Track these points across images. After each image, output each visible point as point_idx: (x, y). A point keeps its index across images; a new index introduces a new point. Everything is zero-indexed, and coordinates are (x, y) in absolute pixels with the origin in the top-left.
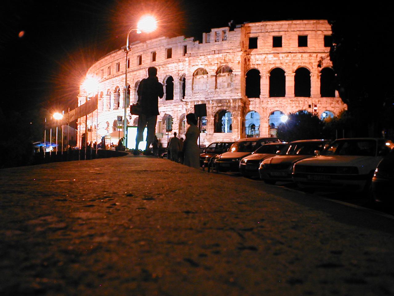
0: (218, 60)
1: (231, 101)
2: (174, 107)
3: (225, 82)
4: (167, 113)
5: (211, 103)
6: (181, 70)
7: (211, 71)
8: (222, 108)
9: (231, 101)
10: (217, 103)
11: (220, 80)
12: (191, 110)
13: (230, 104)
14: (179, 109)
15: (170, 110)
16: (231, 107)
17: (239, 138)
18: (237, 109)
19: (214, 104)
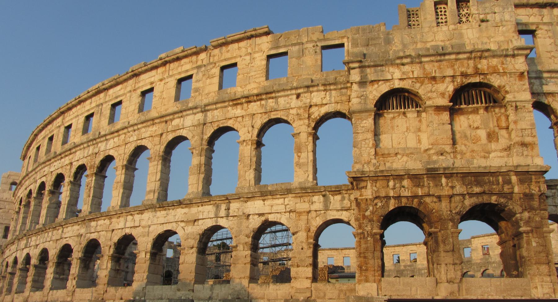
0: (454, 70)
1: (514, 179)
2: (298, 200)
3: (477, 128)
4: (271, 218)
5: (444, 184)
6: (316, 105)
7: (435, 95)
8: (485, 199)
9: (514, 179)
10: (467, 186)
11: (462, 122)
12: (376, 204)
13: (513, 188)
14: (314, 207)
15: (282, 208)
16: (516, 197)
18: (536, 204)
19: (458, 187)
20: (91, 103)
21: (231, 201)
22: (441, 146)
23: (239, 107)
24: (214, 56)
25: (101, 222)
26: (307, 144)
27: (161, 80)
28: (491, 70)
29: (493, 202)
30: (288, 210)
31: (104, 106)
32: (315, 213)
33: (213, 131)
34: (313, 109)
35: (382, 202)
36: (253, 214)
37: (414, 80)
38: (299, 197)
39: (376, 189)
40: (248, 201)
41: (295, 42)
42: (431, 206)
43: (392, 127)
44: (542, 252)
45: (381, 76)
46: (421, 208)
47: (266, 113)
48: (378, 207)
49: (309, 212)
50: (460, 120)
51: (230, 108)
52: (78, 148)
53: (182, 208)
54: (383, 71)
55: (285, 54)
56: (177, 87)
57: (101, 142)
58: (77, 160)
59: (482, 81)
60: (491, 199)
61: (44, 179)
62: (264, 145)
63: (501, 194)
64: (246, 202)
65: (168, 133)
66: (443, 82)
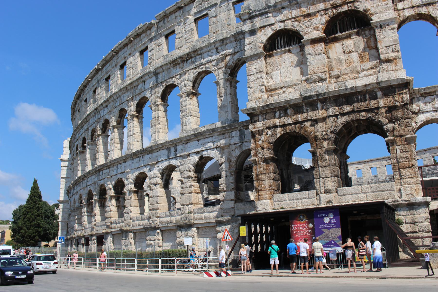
1: (379, 94)
4: (205, 154)
9: (379, 94)
12: (267, 134)
13: (378, 103)
14: (233, 141)
20: (95, 80)
21: (178, 144)
22: (317, 74)
23: (178, 66)
24: (160, 27)
25: (105, 171)
26: (226, 88)
27: (130, 54)
29: (361, 118)
31: (101, 81)
32: (234, 146)
33: (162, 89)
35: (271, 131)
37: (293, 20)
38: (222, 134)
40: (188, 143)
42: (310, 129)
43: (280, 65)
44: (404, 158)
45: (266, 22)
46: (302, 132)
47: (195, 68)
48: (268, 136)
49: (229, 146)
50: (335, 47)
51: (172, 69)
52: (90, 117)
53: (148, 154)
54: (268, 17)
55: (207, 15)
57: (101, 110)
58: (91, 126)
59: (350, 8)
60: (360, 115)
62: (200, 94)
63: (368, 110)
64: (187, 143)
65: (136, 96)
66: (317, 16)
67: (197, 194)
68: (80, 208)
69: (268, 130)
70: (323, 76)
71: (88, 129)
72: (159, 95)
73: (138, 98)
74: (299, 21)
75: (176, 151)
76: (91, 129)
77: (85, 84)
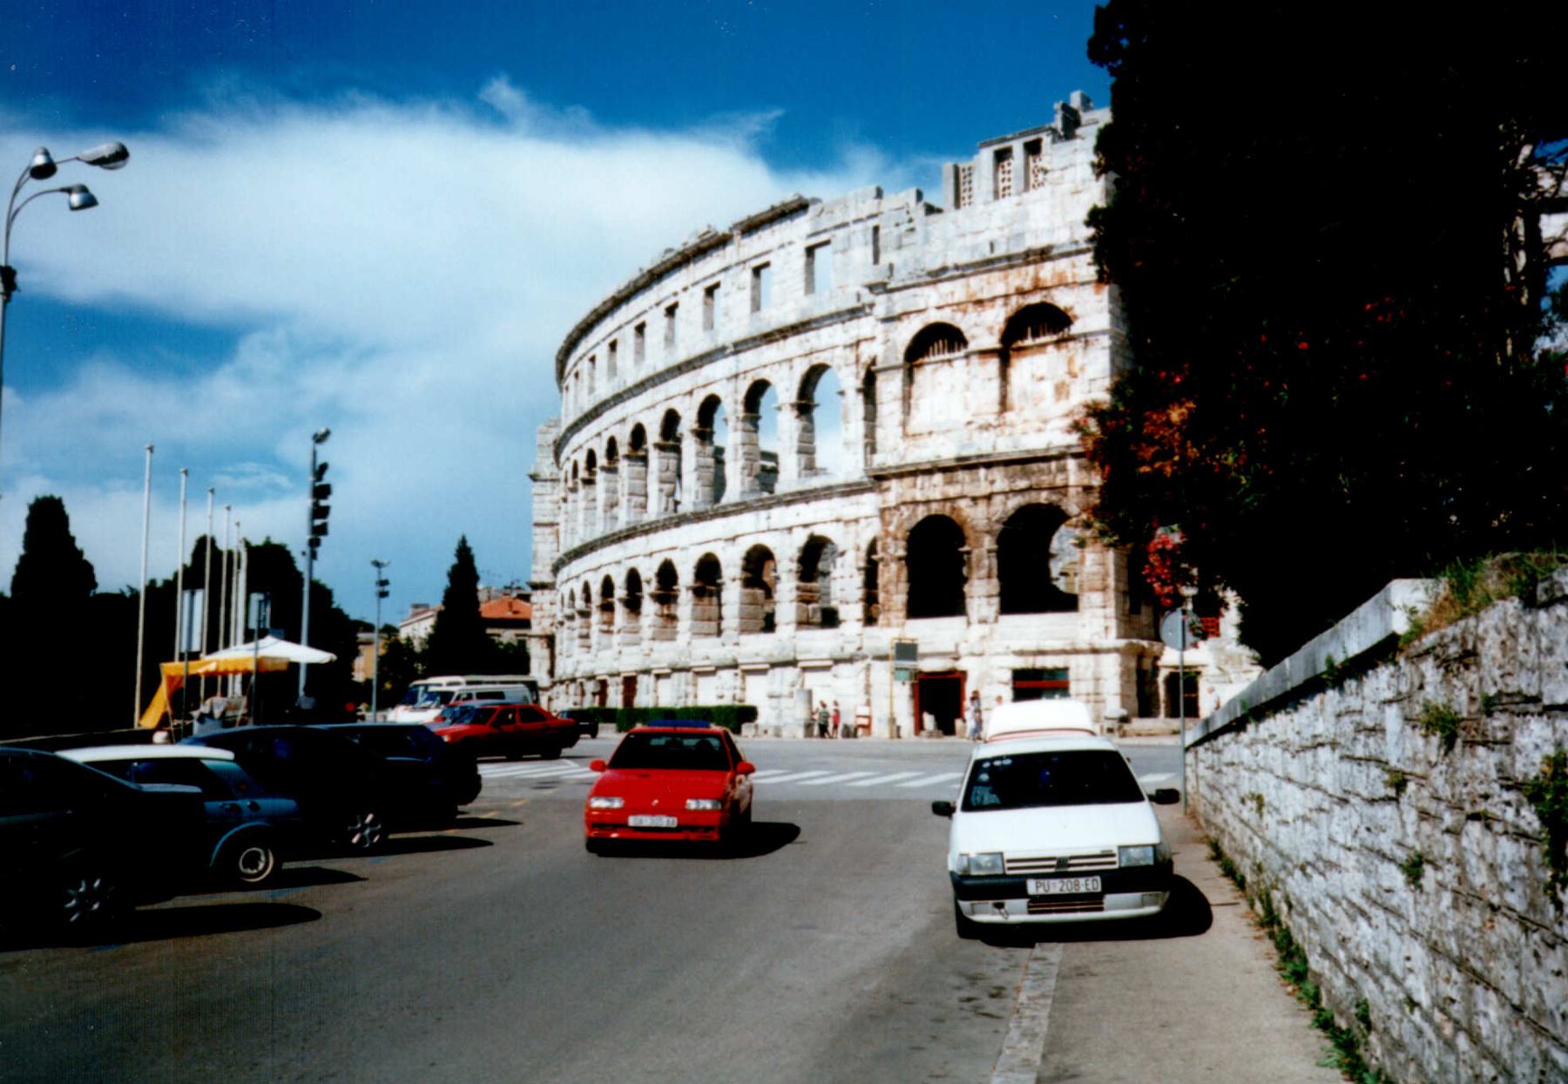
0: (1007, 284)
3: (1042, 379)
4: (819, 531)
6: (866, 340)
8: (1032, 497)
11: (1022, 368)
13: (1067, 479)
15: (827, 515)
16: (1072, 491)
17: (1113, 632)
27: (685, 289)
28: (1056, 282)
30: (833, 518)
34: (864, 347)
36: (798, 526)
37: (955, 308)
39: (901, 491)
41: (839, 222)
46: (954, 517)
55: (827, 243)
56: (706, 303)
59: (1044, 300)
61: (573, 457)
63: (1052, 488)
67: (804, 605)
68: (585, 614)
69: (903, 508)
70: (992, 419)
71: (599, 435)
72: (741, 396)
73: (700, 397)
74: (965, 312)
75: (769, 518)
76: (606, 437)
77: (589, 321)
